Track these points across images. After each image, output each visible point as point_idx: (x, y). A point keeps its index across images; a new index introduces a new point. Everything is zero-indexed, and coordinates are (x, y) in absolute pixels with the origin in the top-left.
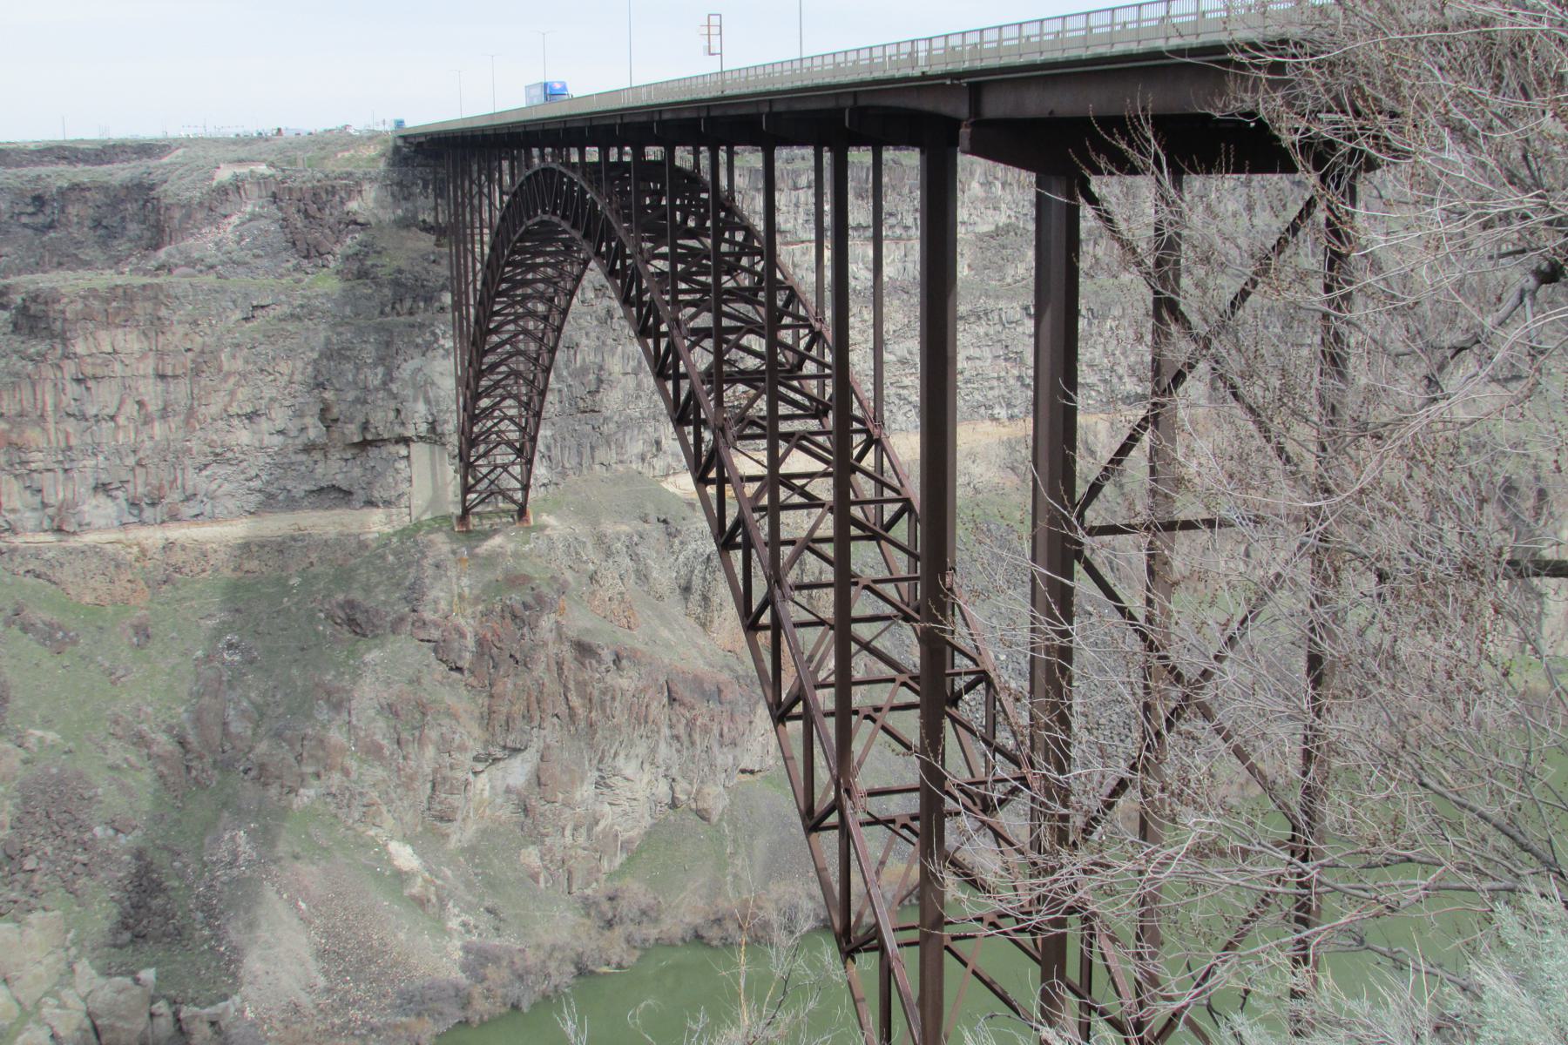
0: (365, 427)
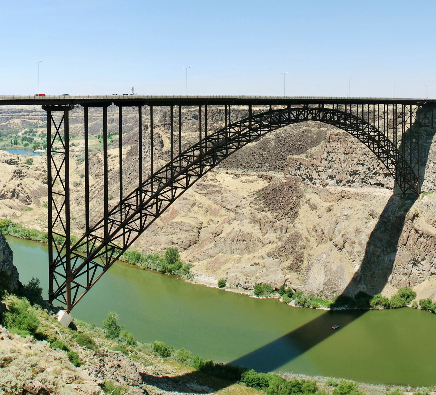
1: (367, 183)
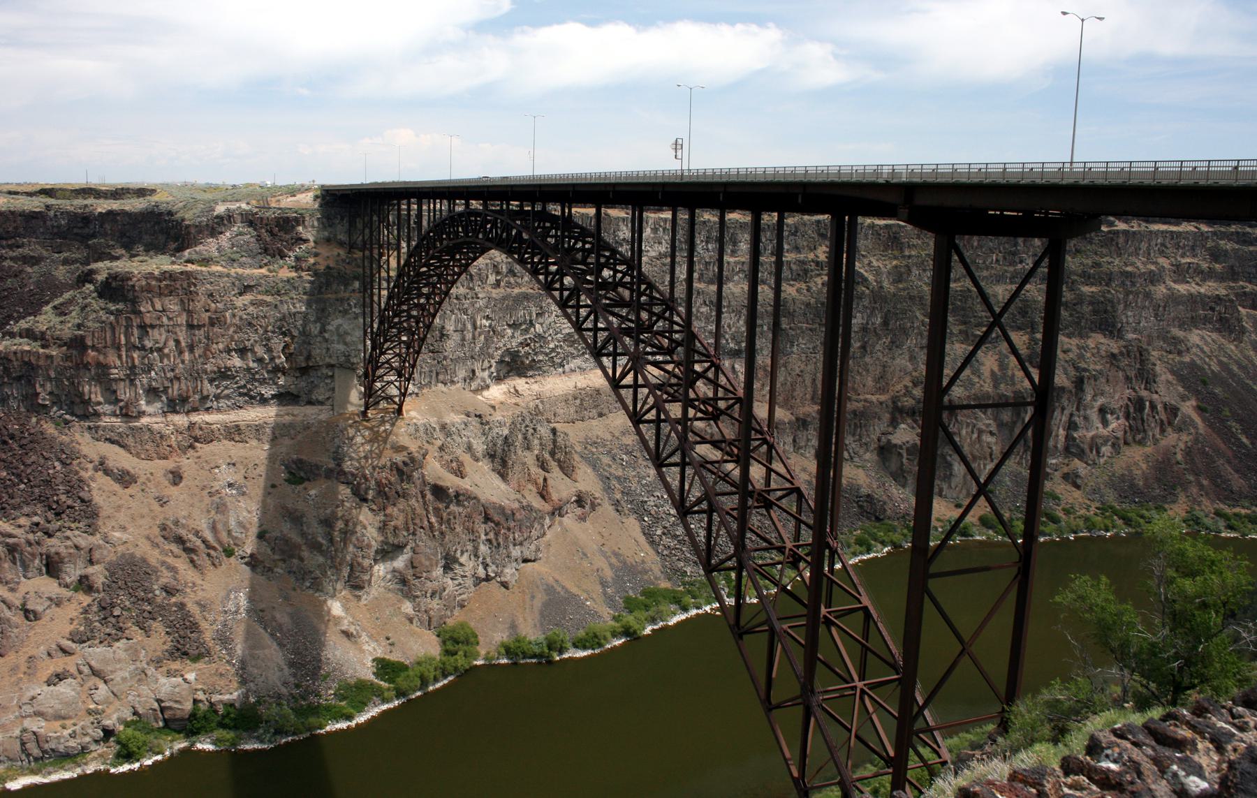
0: (309, 357)
1: (252, 398)
